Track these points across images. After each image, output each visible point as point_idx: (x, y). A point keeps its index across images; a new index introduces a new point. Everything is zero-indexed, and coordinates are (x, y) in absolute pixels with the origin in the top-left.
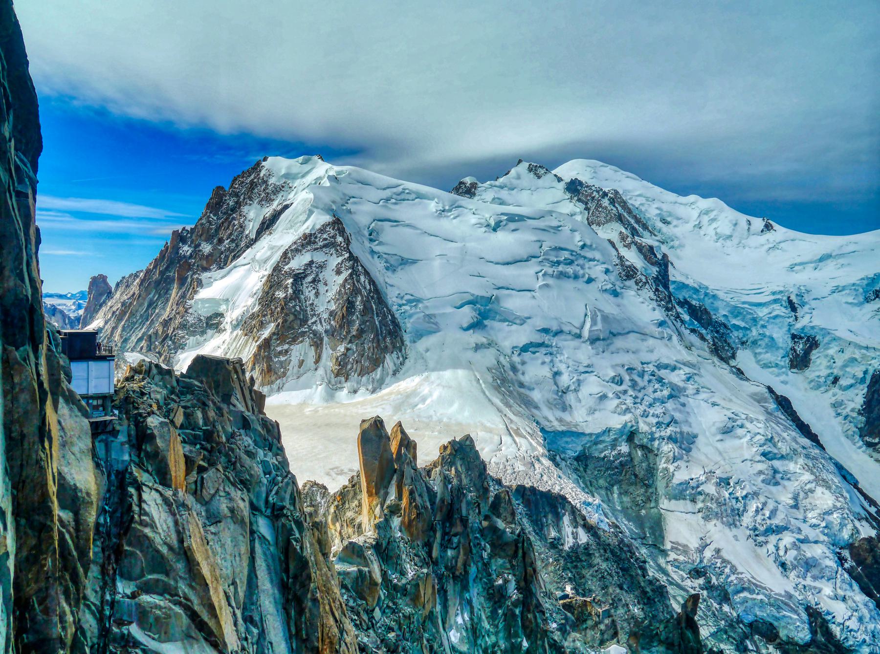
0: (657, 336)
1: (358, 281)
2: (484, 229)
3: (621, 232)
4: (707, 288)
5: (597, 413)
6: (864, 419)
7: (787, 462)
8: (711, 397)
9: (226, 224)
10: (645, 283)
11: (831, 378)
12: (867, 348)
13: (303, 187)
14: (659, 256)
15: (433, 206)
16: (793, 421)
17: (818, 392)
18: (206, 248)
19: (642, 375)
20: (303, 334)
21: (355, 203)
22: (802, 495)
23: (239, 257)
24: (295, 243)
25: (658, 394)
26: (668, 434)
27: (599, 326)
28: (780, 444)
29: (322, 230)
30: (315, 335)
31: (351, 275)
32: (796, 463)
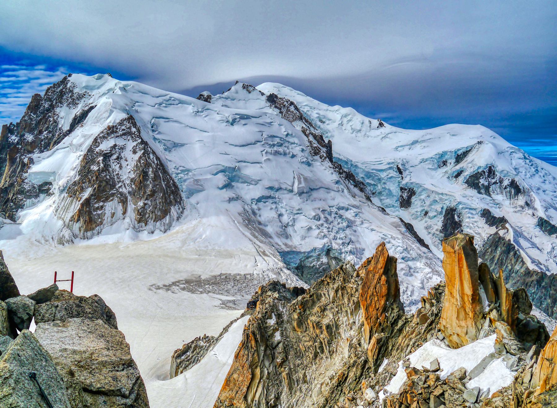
0: (336, 190)
1: (149, 158)
2: (225, 124)
3: (303, 127)
4: (351, 161)
5: (307, 239)
6: (443, 235)
7: (415, 262)
8: (370, 226)
9: (44, 121)
10: (326, 158)
11: (424, 212)
12: (442, 194)
13: (99, 95)
14: (326, 142)
15: (190, 109)
16: (415, 237)
17: (417, 221)
18: (30, 138)
19: (330, 214)
20: (113, 195)
21: (139, 106)
22: (425, 281)
23: (59, 142)
24: (102, 132)
25: (341, 226)
26: (349, 249)
27: (303, 185)
28: (411, 252)
29: (121, 123)
30: (121, 195)
31: (144, 154)
32: (421, 262)
